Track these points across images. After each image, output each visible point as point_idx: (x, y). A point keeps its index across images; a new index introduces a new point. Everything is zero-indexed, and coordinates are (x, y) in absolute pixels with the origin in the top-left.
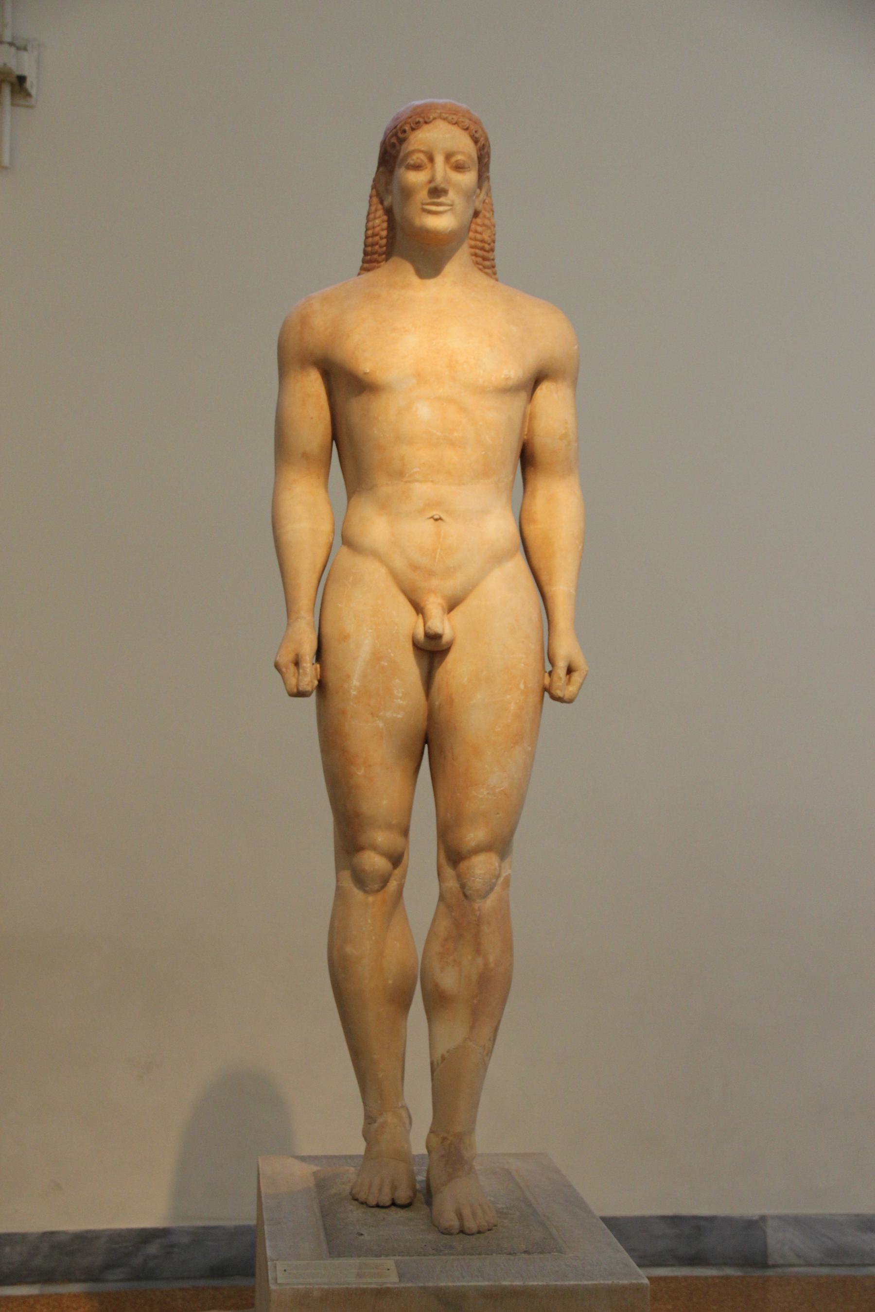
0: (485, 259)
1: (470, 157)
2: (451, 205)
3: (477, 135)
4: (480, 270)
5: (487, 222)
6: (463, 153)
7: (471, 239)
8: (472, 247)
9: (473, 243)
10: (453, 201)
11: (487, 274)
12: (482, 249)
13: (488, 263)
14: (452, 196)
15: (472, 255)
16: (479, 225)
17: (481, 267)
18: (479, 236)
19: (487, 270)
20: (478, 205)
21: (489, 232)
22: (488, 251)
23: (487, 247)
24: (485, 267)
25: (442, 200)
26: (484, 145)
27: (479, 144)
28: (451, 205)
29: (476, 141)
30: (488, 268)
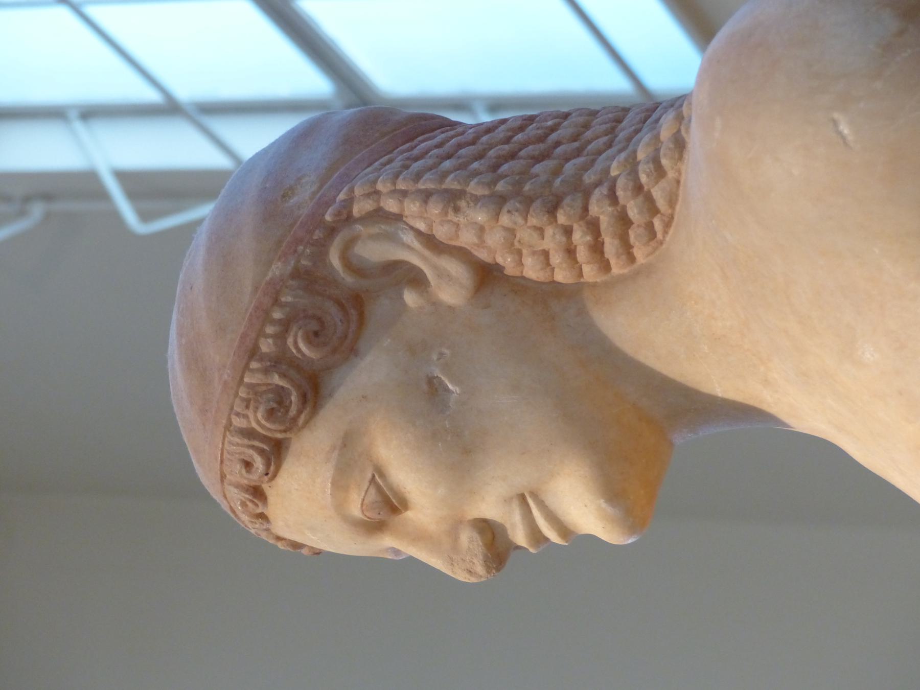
0: (624, 221)
1: (340, 484)
2: (522, 498)
3: (259, 463)
4: (667, 225)
5: (495, 239)
6: (340, 508)
7: (581, 275)
8: (605, 266)
9: (590, 273)
10: (507, 501)
11: (672, 202)
12: (597, 248)
13: (634, 212)
14: (489, 507)
15: (632, 259)
16: (520, 264)
17: (657, 223)
18: (556, 259)
19: (661, 203)
20: (451, 287)
21: (525, 235)
22: (594, 227)
23: (580, 237)
24: (652, 208)
25: (520, 537)
26: (271, 414)
27: (279, 436)
28: (522, 498)
29: (276, 452)
30: (650, 200)
